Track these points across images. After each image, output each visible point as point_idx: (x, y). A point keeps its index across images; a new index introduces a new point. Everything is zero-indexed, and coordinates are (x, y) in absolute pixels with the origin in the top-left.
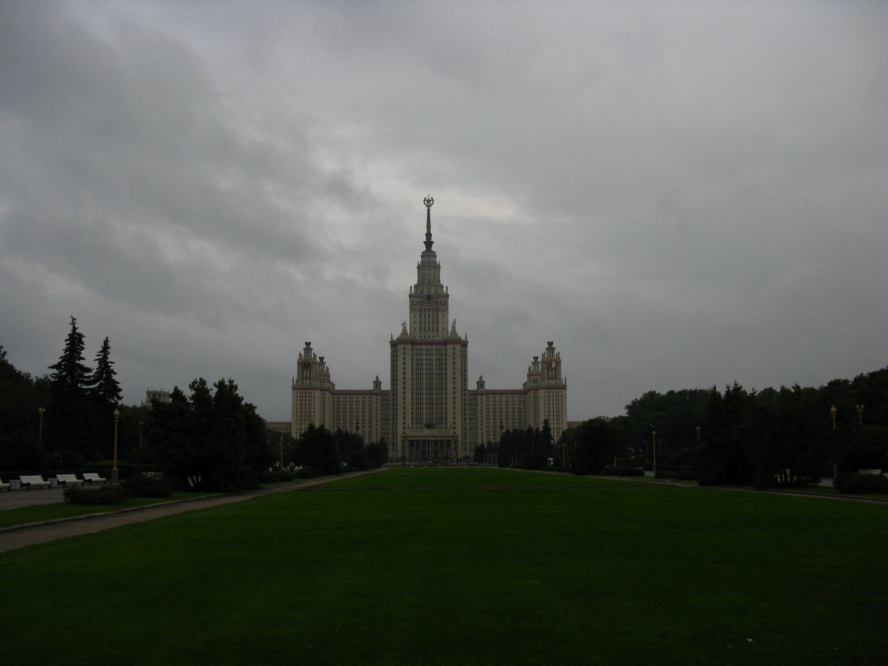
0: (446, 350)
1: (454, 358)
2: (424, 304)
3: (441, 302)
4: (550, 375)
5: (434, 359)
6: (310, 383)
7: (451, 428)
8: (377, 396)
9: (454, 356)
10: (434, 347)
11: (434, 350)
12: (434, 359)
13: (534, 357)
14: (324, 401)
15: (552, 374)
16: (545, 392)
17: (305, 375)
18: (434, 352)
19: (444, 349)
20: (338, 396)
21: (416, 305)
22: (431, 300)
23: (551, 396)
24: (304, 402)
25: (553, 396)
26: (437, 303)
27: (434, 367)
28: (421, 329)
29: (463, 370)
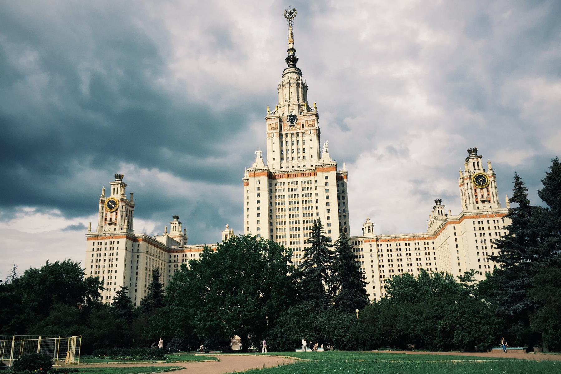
0: (316, 181)
3: (307, 121)
4: (479, 196)
6: (115, 229)
9: (327, 187)
10: (299, 180)
13: (436, 201)
14: (138, 256)
15: (482, 196)
16: (474, 222)
17: (108, 219)
19: (313, 182)
20: (176, 254)
22: (295, 123)
25: (489, 228)
26: (303, 125)
28: (282, 159)
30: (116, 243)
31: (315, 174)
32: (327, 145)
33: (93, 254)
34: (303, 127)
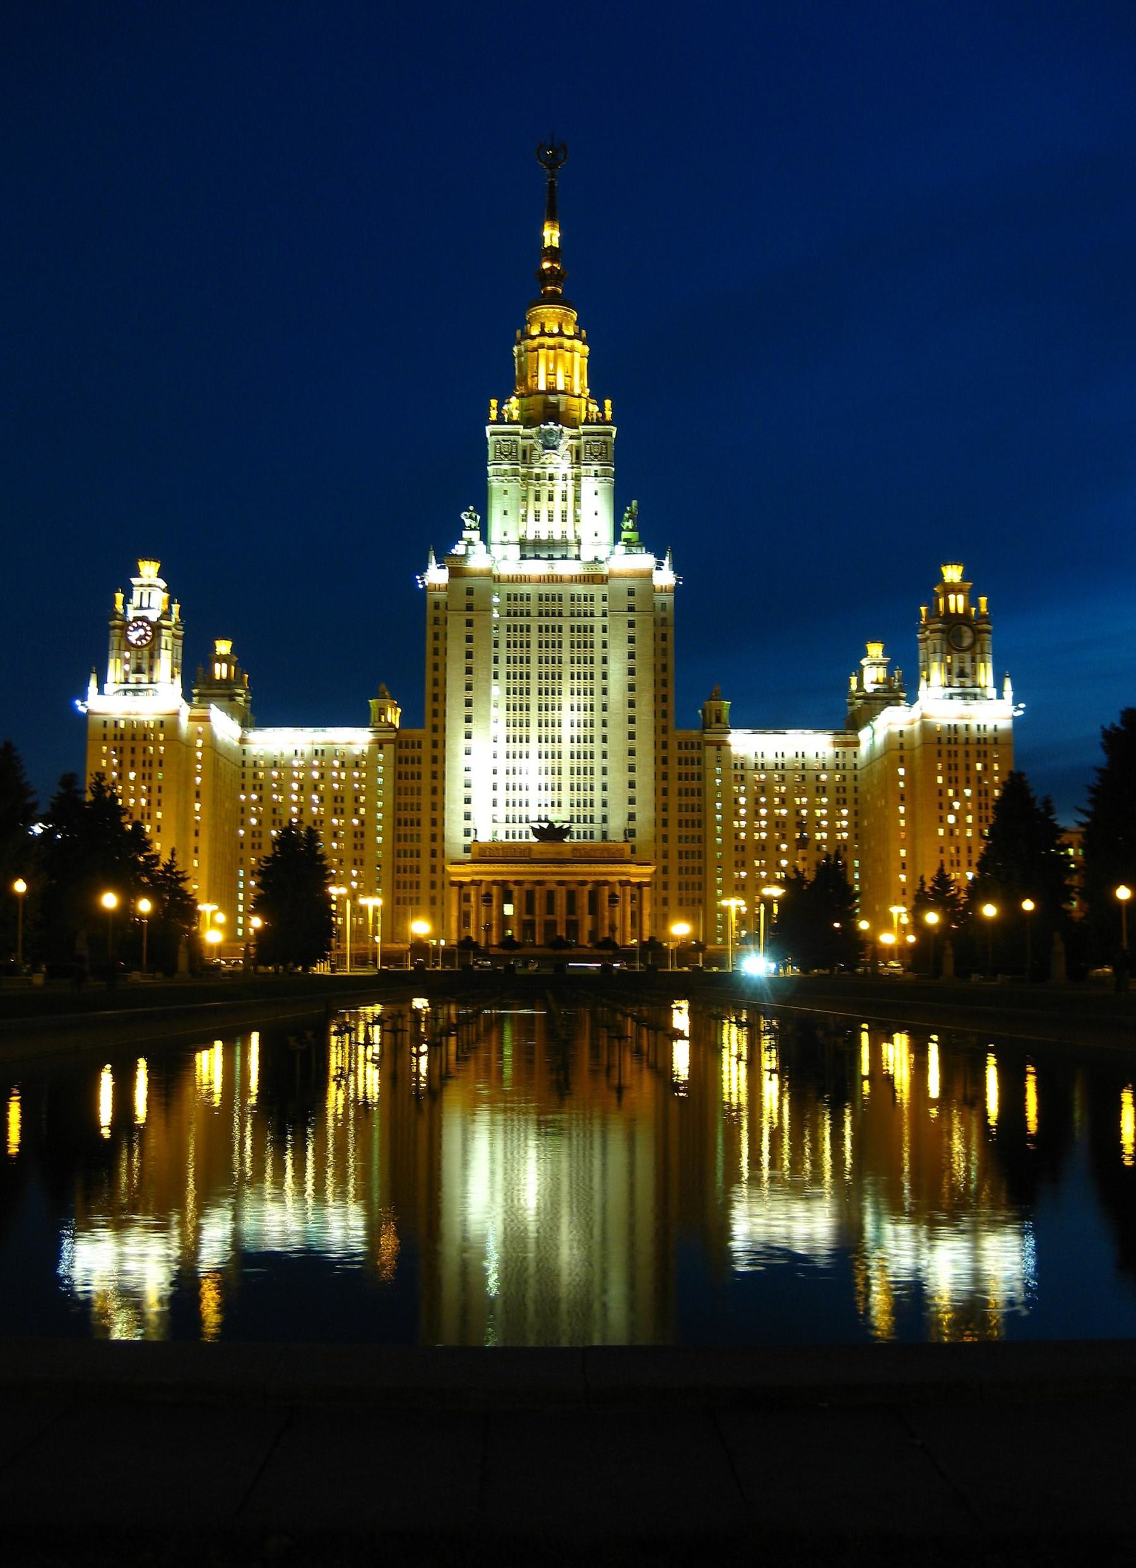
7: (626, 841)
9: (631, 616)
26: (578, 453)
27: (566, 657)
29: (659, 667)
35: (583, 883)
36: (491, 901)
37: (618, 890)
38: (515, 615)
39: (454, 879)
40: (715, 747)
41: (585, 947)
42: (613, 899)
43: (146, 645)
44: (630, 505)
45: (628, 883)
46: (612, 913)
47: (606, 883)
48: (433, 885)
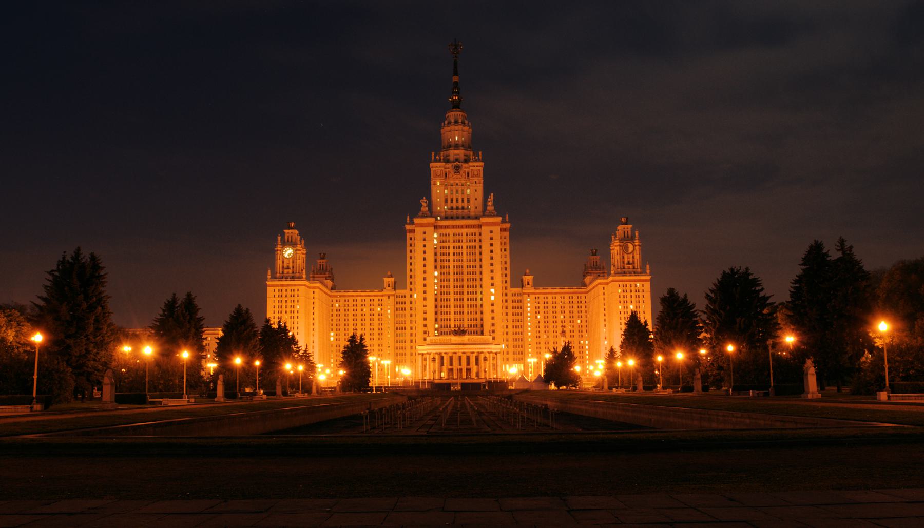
0: (480, 234)
1: (491, 245)
2: (450, 174)
5: (465, 247)
7: (490, 335)
8: (389, 298)
9: (491, 242)
10: (464, 231)
11: (464, 235)
12: (465, 247)
14: (314, 302)
18: (464, 237)
21: (440, 177)
23: (628, 291)
24: (284, 304)
26: (468, 174)
27: (465, 259)
30: (296, 290)
31: (480, 226)
32: (492, 198)
33: (274, 301)
34: (468, 176)
35: (473, 353)
36: (435, 361)
37: (487, 356)
38: (443, 242)
39: (420, 352)
40: (527, 295)
41: (474, 379)
42: (485, 359)
43: (291, 258)
44: (491, 195)
45: (491, 352)
46: (485, 366)
47: (482, 353)
48: (411, 354)
